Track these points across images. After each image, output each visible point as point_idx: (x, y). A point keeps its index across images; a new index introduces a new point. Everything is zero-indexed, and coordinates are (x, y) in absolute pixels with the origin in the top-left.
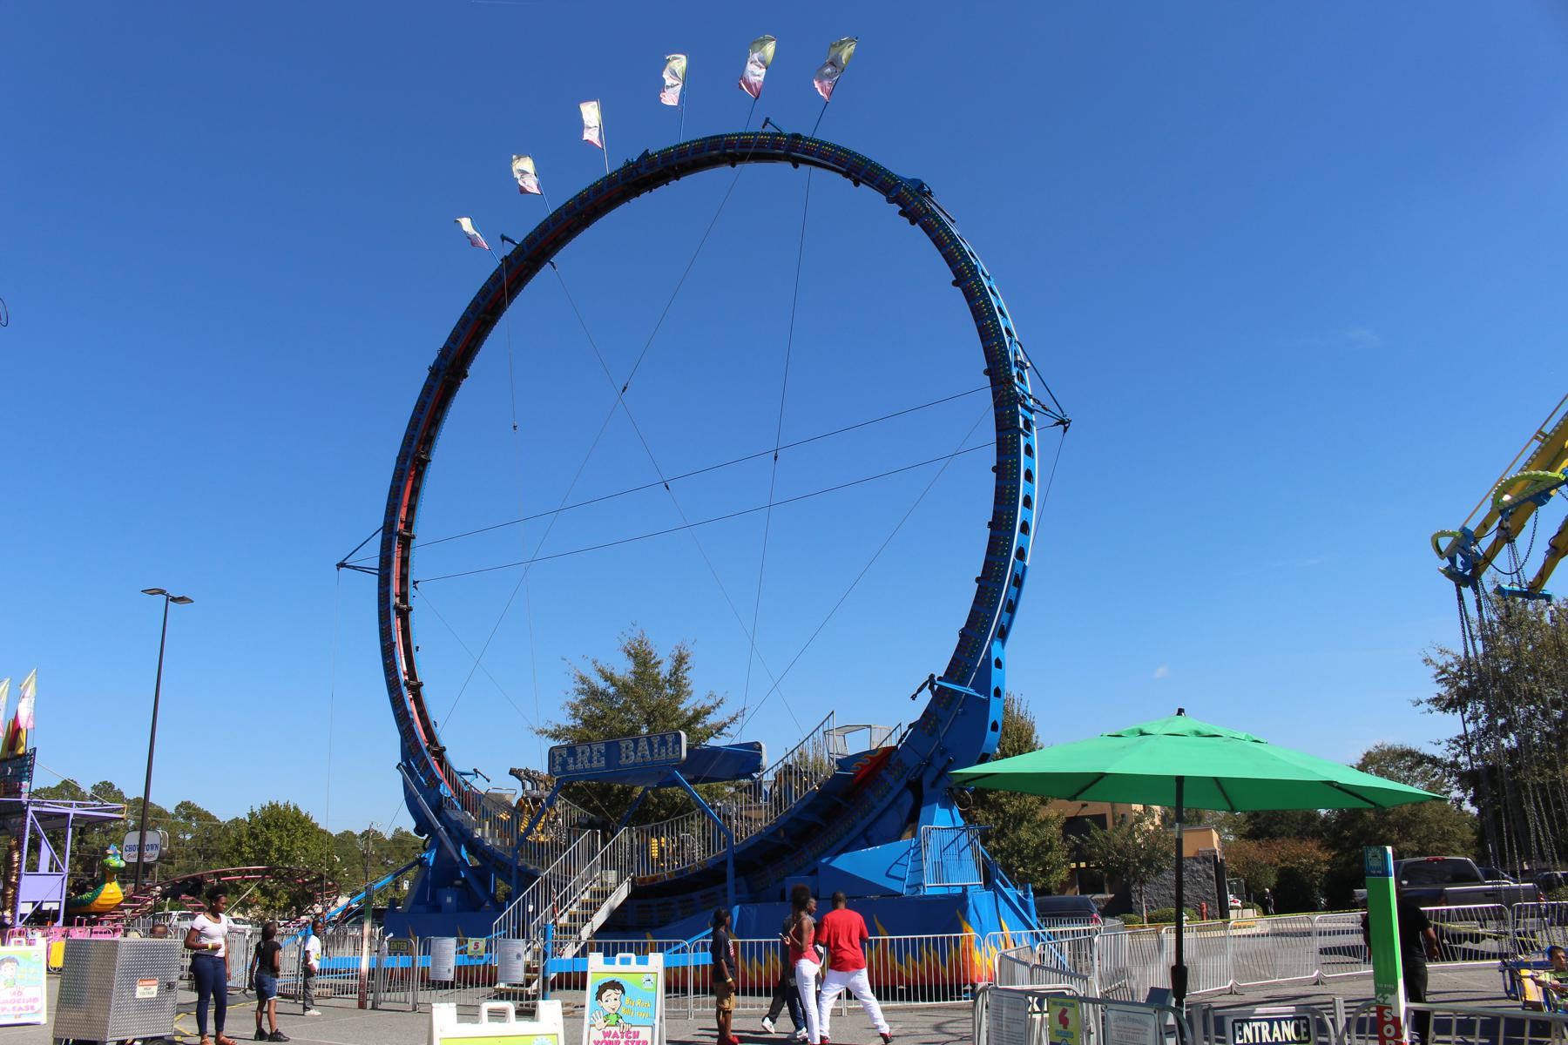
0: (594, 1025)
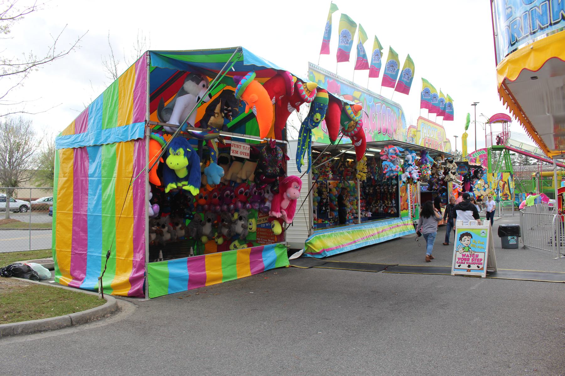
0: (458, 251)
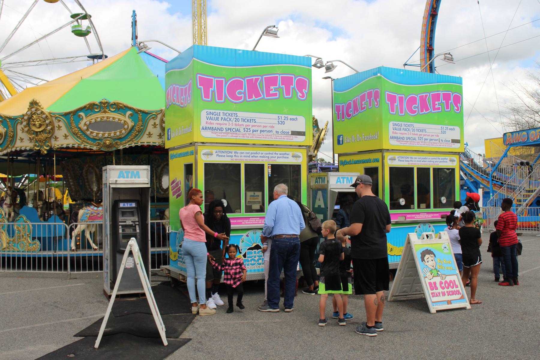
0: (426, 277)
